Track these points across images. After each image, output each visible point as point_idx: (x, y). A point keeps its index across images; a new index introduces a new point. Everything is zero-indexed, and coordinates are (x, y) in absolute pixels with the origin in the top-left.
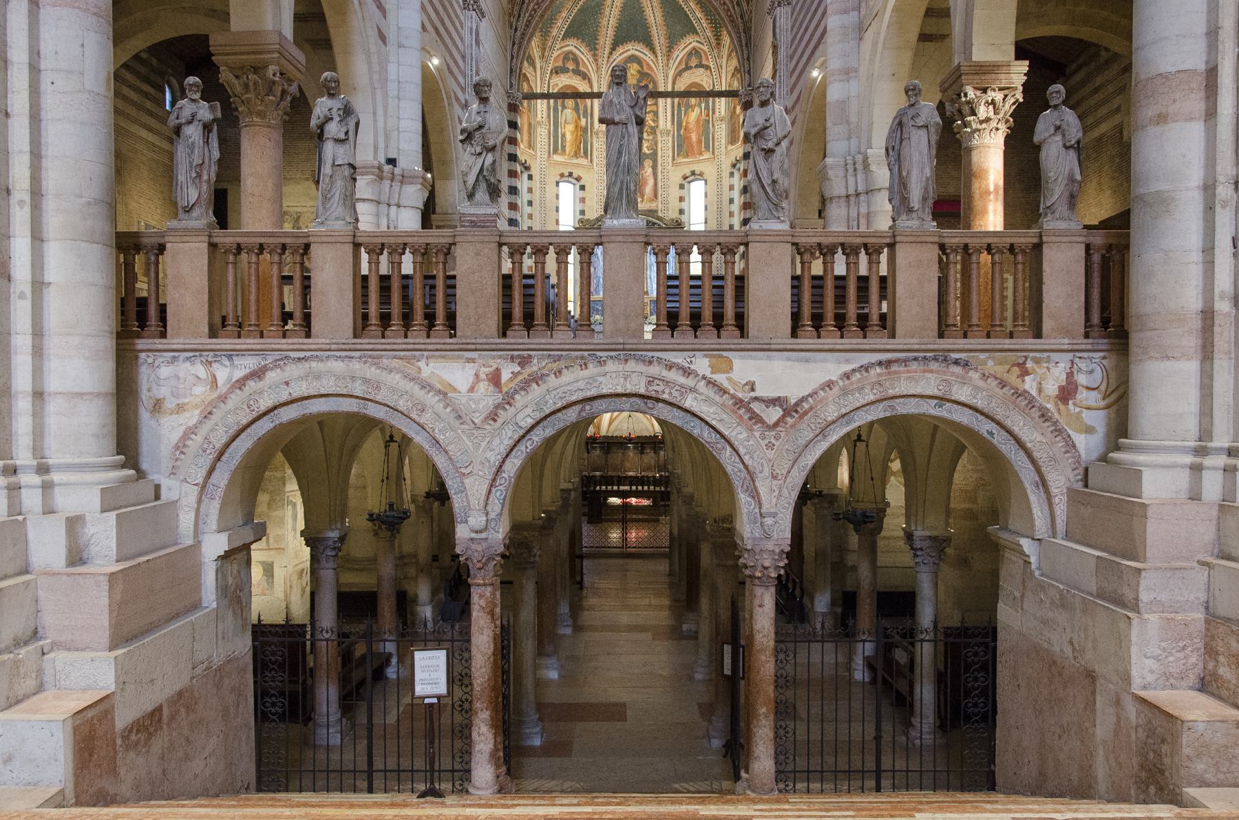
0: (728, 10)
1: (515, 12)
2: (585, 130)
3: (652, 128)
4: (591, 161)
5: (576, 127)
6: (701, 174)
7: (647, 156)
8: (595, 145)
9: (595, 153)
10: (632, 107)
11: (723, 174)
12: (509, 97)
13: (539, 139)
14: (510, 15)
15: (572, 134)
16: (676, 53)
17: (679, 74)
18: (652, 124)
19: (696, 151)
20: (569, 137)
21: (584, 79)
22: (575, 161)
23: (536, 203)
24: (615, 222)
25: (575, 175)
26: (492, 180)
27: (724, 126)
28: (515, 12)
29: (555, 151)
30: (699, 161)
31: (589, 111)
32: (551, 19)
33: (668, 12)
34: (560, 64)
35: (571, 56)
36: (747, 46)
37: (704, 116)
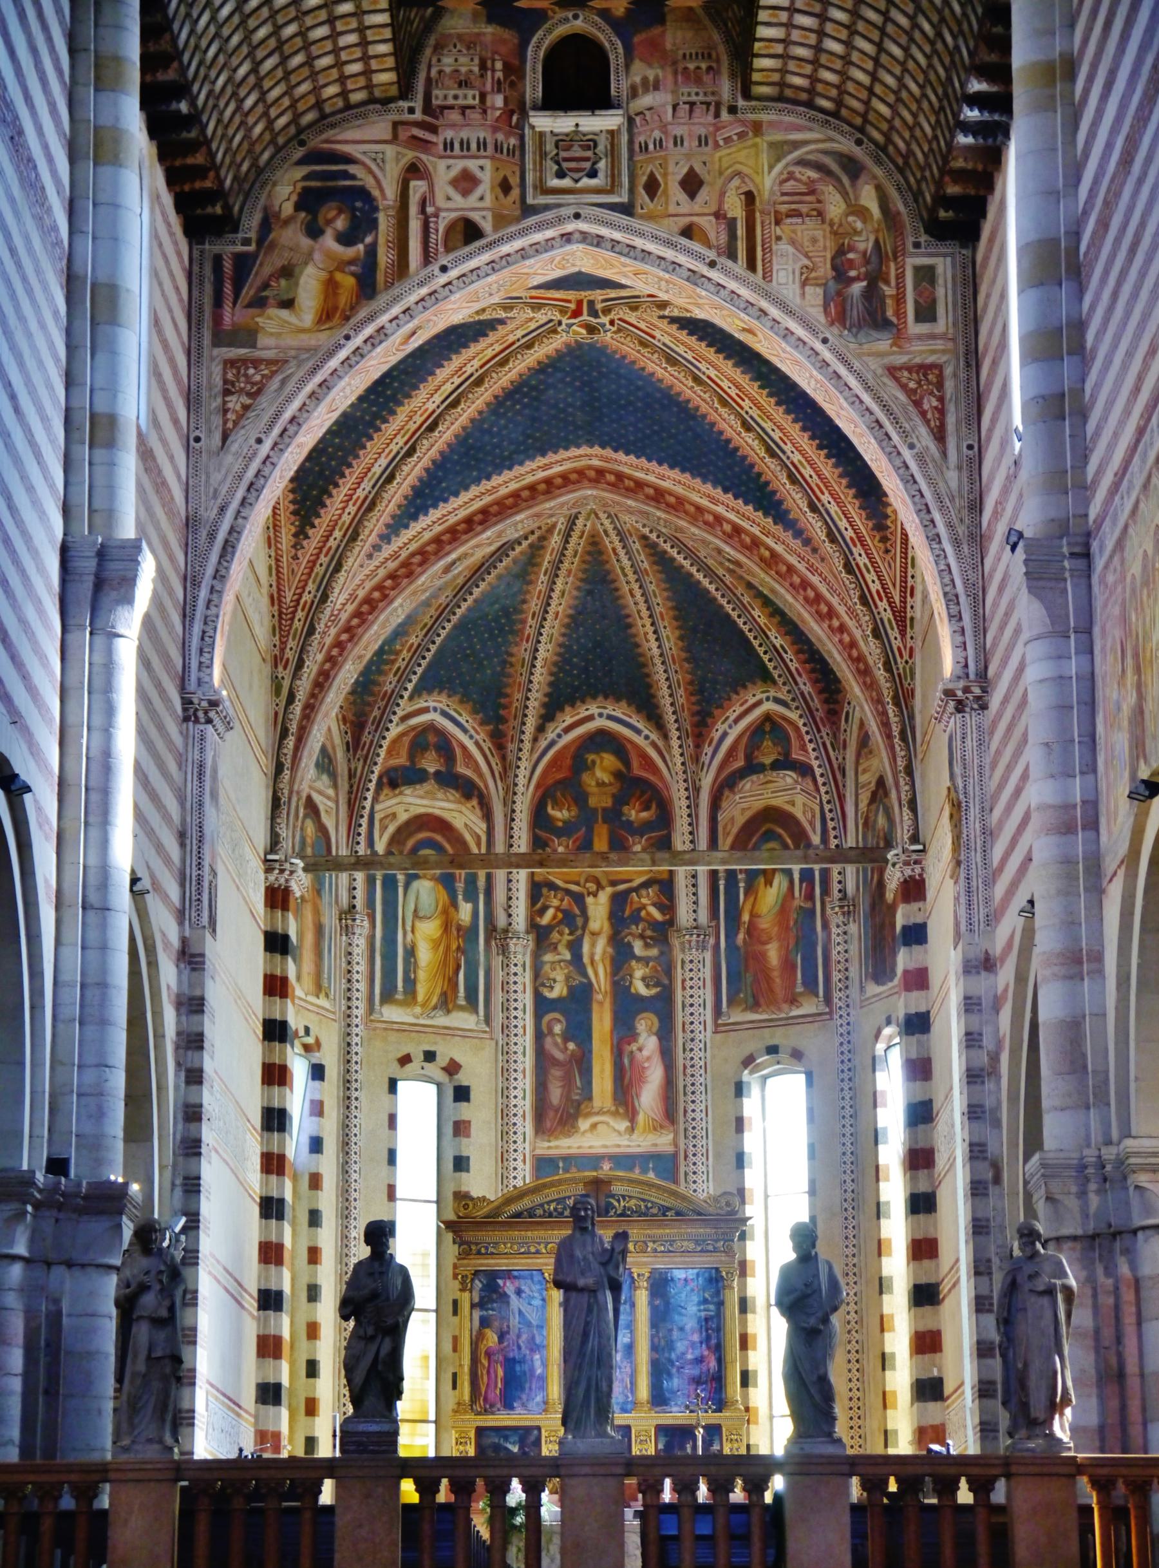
0: (853, 644)
1: (289, 654)
2: (470, 933)
3: (654, 925)
4: (488, 1020)
5: (446, 927)
8: (499, 975)
9: (498, 997)
10: (604, 1264)
12: (268, 870)
14: (276, 662)
15: (436, 944)
16: (721, 727)
17: (726, 784)
18: (657, 915)
20: (425, 955)
21: (467, 796)
22: (442, 1020)
24: (578, 1441)
26: (391, 1377)
27: (853, 928)
29: (388, 996)
30: (790, 1021)
34: (402, 760)
35: (432, 738)
36: (904, 738)
37: (798, 900)
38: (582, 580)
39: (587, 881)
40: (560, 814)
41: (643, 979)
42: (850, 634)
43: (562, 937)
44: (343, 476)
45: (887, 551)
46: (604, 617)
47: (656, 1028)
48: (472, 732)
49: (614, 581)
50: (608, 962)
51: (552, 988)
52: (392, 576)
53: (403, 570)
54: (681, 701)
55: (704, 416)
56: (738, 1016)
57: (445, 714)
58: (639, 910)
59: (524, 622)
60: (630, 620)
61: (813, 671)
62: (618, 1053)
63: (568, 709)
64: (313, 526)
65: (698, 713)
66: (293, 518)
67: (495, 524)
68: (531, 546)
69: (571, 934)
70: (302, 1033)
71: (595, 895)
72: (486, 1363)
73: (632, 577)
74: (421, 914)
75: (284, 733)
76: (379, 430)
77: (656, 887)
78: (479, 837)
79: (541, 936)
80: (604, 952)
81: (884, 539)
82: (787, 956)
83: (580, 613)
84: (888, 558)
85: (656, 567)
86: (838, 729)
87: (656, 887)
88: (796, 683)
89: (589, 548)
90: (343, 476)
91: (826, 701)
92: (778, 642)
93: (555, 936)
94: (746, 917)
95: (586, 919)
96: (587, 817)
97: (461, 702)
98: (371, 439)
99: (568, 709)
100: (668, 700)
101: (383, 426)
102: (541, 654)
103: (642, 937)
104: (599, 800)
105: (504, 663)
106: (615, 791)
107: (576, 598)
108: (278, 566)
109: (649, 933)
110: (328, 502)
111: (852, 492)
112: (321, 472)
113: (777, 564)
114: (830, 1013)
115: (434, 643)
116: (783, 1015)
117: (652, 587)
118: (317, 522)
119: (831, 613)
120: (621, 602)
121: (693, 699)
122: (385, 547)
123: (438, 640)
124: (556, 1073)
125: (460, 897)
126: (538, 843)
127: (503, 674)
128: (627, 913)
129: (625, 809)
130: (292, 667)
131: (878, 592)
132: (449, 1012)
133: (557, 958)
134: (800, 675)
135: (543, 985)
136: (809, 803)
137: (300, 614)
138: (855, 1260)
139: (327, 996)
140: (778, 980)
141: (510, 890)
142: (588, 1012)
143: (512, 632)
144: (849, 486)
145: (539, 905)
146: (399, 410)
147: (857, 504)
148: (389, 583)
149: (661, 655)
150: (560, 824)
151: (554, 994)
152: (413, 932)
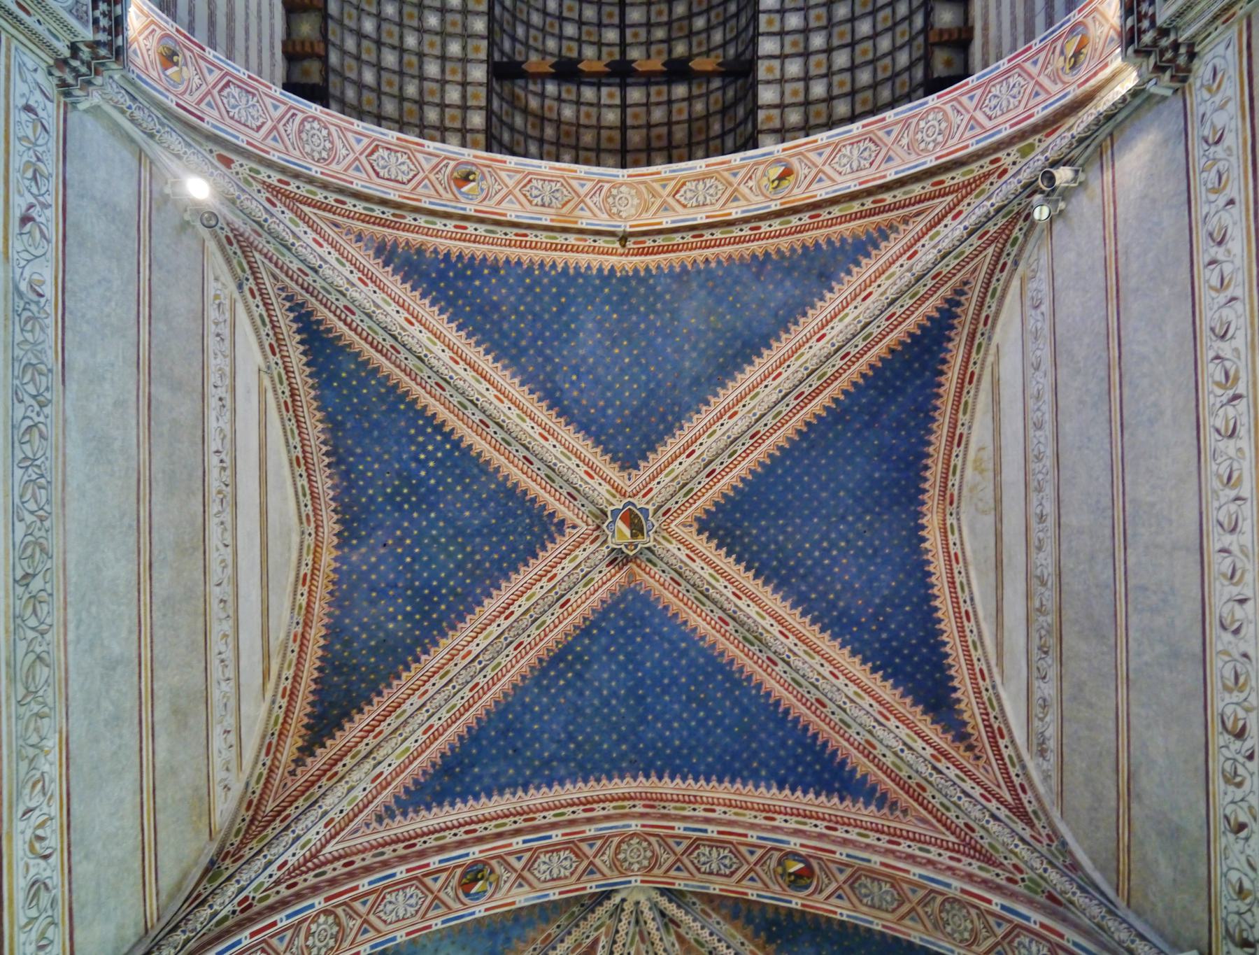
44: (370, 703)
45: (978, 758)
55: (749, 678)
64: (323, 746)
66: (303, 731)
76: (417, 660)
81: (970, 748)
84: (981, 762)
90: (370, 703)
98: (408, 669)
101: (423, 657)
108: (269, 776)
110: (347, 726)
111: (920, 708)
112: (348, 691)
118: (329, 743)
122: (399, 818)
144: (915, 704)
146: (443, 641)
147: (929, 719)
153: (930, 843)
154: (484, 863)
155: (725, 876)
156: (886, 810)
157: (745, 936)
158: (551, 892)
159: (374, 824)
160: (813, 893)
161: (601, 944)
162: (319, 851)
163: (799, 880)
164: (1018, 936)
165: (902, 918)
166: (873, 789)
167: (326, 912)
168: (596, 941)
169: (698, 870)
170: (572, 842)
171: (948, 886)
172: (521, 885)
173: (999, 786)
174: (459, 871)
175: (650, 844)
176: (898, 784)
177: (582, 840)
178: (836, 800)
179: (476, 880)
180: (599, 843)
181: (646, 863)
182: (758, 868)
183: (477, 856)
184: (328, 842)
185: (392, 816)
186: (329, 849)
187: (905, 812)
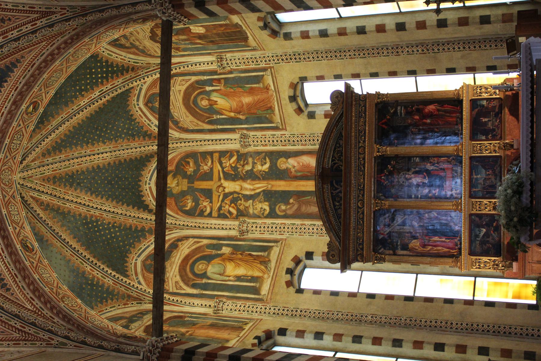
0: (65, 42)
1: (46, 337)
2: (236, 248)
3: (238, 160)
4: (276, 241)
5: (231, 260)
6: (294, 86)
7: (273, 165)
8: (257, 235)
9: (267, 236)
11: (290, 51)
13: (236, 314)
14: (49, 345)
15: (238, 265)
18: (235, 158)
19: (264, 96)
22: (273, 264)
23: (320, 326)
25: (291, 265)
27: (229, 55)
28: (47, 336)
29: (256, 291)
30: (277, 91)
31: (215, 242)
32: (92, 285)
33: (100, 136)
38: (71, 187)
39: (218, 192)
40: (190, 204)
41: (262, 165)
42: (61, 44)
43: (242, 204)
46: (94, 178)
47: (284, 160)
48: (150, 243)
49: (73, 173)
50: (254, 182)
51: (265, 210)
52: (24, 278)
53: (22, 272)
54: (136, 144)
56: (277, 118)
57: (139, 256)
58: (232, 167)
59: (92, 216)
60: (95, 166)
61: (112, 78)
62: (296, 178)
63: (144, 198)
65: (144, 137)
67: (5, 224)
68: (45, 210)
69: (241, 200)
70: (256, 341)
71: (225, 188)
72: (430, 247)
73: (67, 163)
74: (222, 272)
75: (84, 343)
77: (222, 159)
78: (195, 242)
79: (242, 214)
80: (250, 184)
82: (247, 92)
83: (90, 189)
84: (13, 19)
85: (63, 152)
86: (141, 66)
87: (222, 159)
88: (117, 85)
89: (51, 182)
91: (127, 71)
92: (97, 94)
93: (241, 207)
94: (232, 114)
95: (235, 192)
96: (191, 191)
97: (134, 247)
99: (144, 198)
100: (134, 150)
102: (108, 209)
103: (243, 166)
104: (184, 185)
105: (113, 226)
106: (181, 178)
107: (81, 191)
109: (242, 163)
113: (30, 82)
114: (270, 68)
115: (89, 259)
116: (274, 93)
117: (76, 154)
119: (52, 54)
120: (84, 169)
121: (137, 139)
122: (5, 282)
123: (88, 256)
124: (303, 209)
125: (219, 252)
126: (201, 214)
127: (119, 227)
128: (233, 173)
129: (189, 173)
130: (53, 337)
131: (32, 26)
132: (269, 261)
133: (251, 207)
134: (114, 84)
135: (263, 214)
136: (178, 82)
137: (27, 329)
138: (390, 48)
139: (246, 324)
140: (259, 97)
141: (219, 228)
142: (276, 192)
143: (97, 221)
145: (228, 215)
148: (27, 280)
149: (111, 152)
150: (194, 204)
151: (268, 208)
152: (229, 276)
153: (41, 52)
154: (21, 243)
155: (23, 138)
156: (18, 65)
157: (39, 133)
158: (23, 215)
159: (11, 291)
160: (42, 103)
161: (33, 195)
162: (32, 311)
163: (35, 109)
164: (100, 36)
165: (66, 71)
166: (7, 67)
167: (63, 302)
168: (32, 197)
169: (18, 149)
170: (5, 204)
171: (70, 52)
172: (24, 227)
173: (29, 17)
174: (27, 253)
175: (4, 170)
176: (10, 56)
177: (4, 200)
178: (5, 84)
179: (27, 246)
180: (4, 193)
181: (10, 172)
182: (25, 124)
183: (19, 246)
184: (27, 308)
185: (6, 285)
186: (29, 307)
187: (22, 57)
